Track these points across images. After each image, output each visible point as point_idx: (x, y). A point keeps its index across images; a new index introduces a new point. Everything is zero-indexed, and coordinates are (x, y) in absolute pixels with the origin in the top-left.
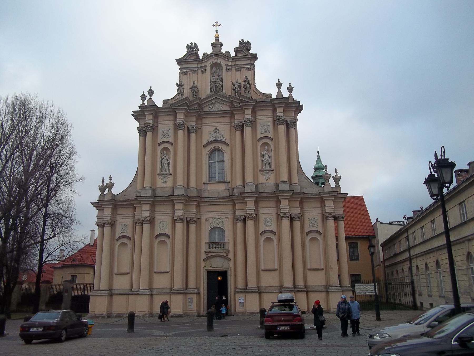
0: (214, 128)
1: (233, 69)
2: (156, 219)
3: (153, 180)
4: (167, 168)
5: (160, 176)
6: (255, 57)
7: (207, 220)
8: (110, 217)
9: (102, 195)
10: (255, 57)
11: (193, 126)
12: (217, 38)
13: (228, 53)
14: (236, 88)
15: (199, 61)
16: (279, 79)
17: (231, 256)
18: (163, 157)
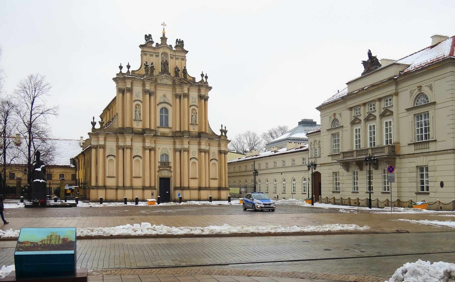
0: (163, 94)
1: (174, 57)
2: (133, 147)
3: (132, 123)
4: (139, 117)
5: (135, 121)
6: (187, 52)
7: (159, 149)
8: (103, 143)
9: (93, 129)
10: (187, 52)
11: (153, 92)
12: (164, 35)
13: (171, 46)
14: (177, 71)
15: (155, 49)
16: (202, 72)
17: (172, 170)
18: (137, 109)
